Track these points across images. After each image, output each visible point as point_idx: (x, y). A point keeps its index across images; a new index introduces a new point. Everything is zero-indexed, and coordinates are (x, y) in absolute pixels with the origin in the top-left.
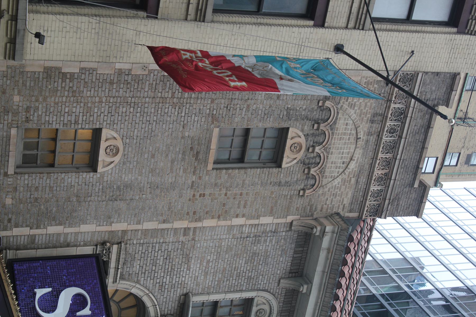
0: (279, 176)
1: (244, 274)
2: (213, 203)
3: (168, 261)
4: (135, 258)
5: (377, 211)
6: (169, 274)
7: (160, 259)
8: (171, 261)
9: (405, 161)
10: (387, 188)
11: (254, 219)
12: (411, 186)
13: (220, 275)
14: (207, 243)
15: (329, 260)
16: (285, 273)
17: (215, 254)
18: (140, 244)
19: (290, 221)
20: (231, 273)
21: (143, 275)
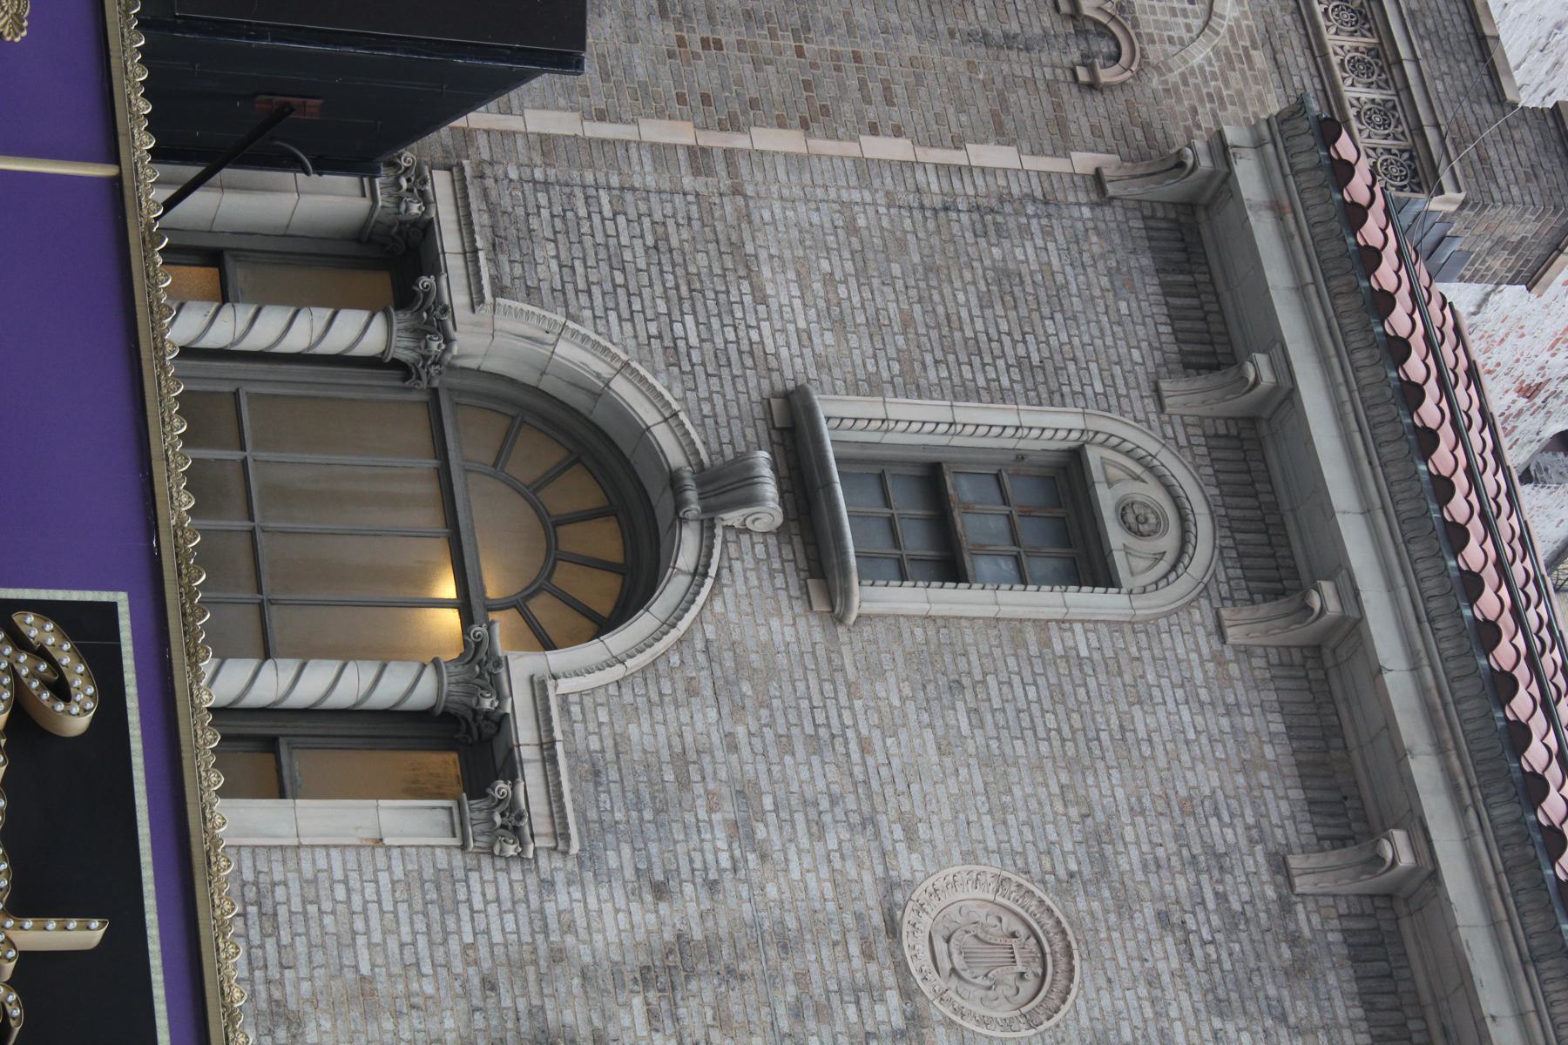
0: (970, 11)
1: (994, 345)
2: (761, 75)
3: (665, 259)
4: (530, 231)
5: (1415, 173)
6: (687, 306)
7: (632, 247)
8: (678, 258)
9: (1418, 15)
10: (1403, 95)
11: (943, 147)
12: (1494, 99)
13: (900, 340)
14: (795, 211)
15: (1297, 239)
16: (1166, 363)
17: (846, 255)
18: (535, 182)
19: (1091, 171)
20: (941, 337)
21: (583, 298)
